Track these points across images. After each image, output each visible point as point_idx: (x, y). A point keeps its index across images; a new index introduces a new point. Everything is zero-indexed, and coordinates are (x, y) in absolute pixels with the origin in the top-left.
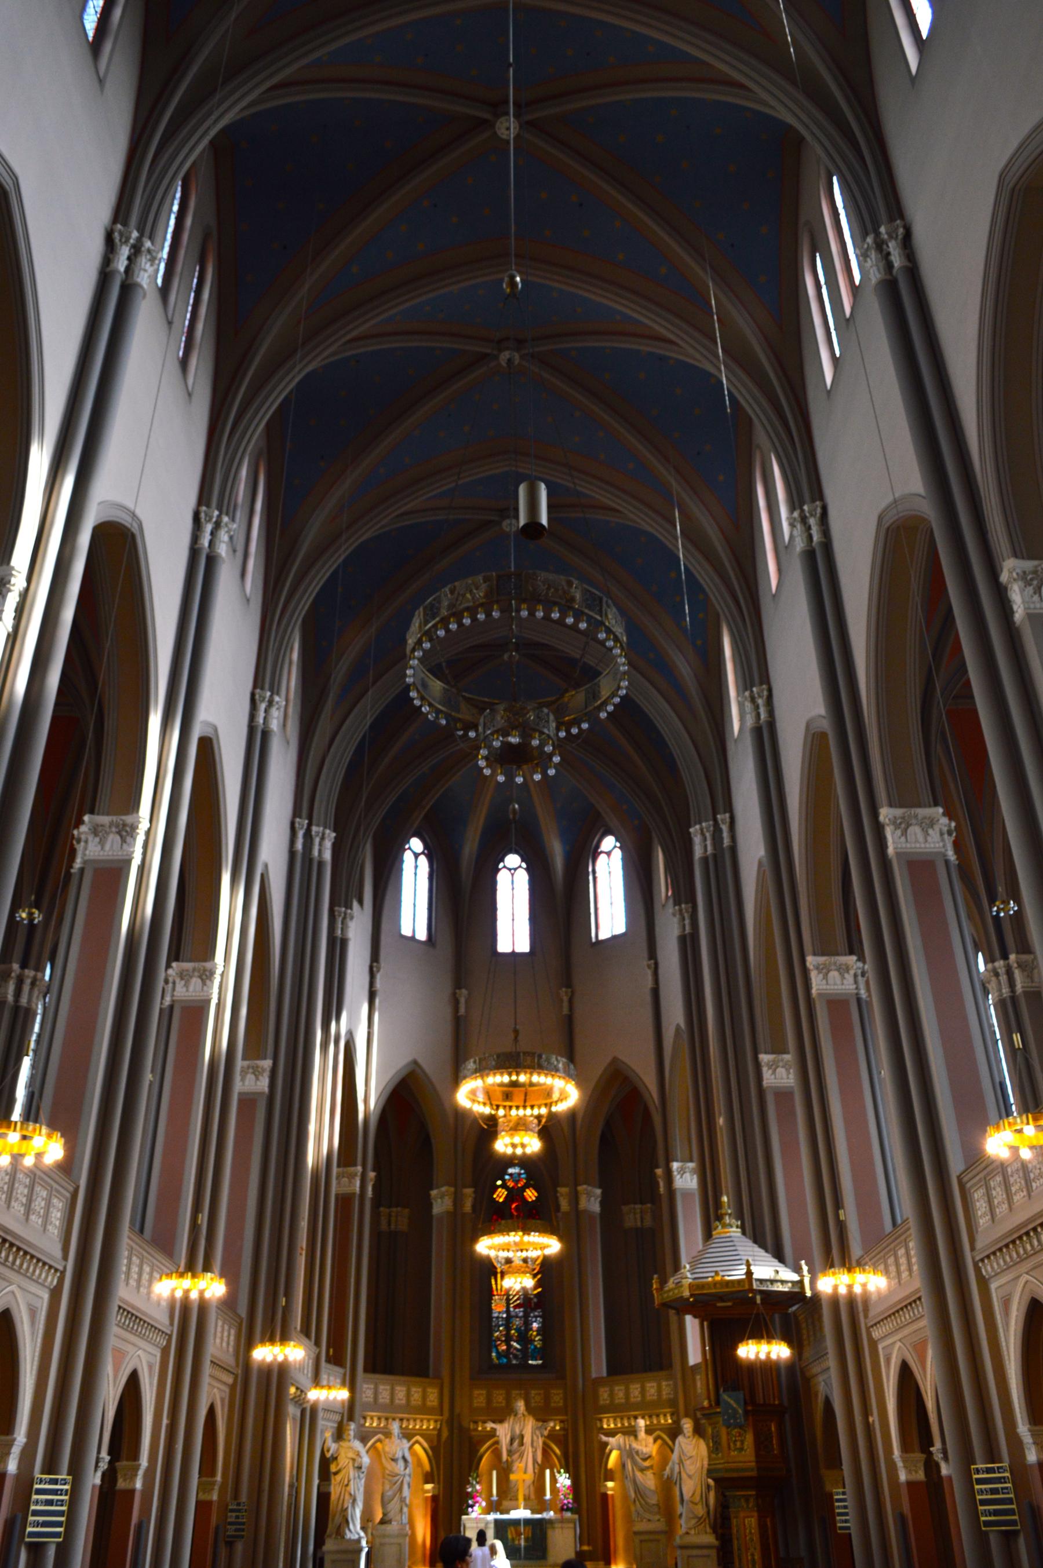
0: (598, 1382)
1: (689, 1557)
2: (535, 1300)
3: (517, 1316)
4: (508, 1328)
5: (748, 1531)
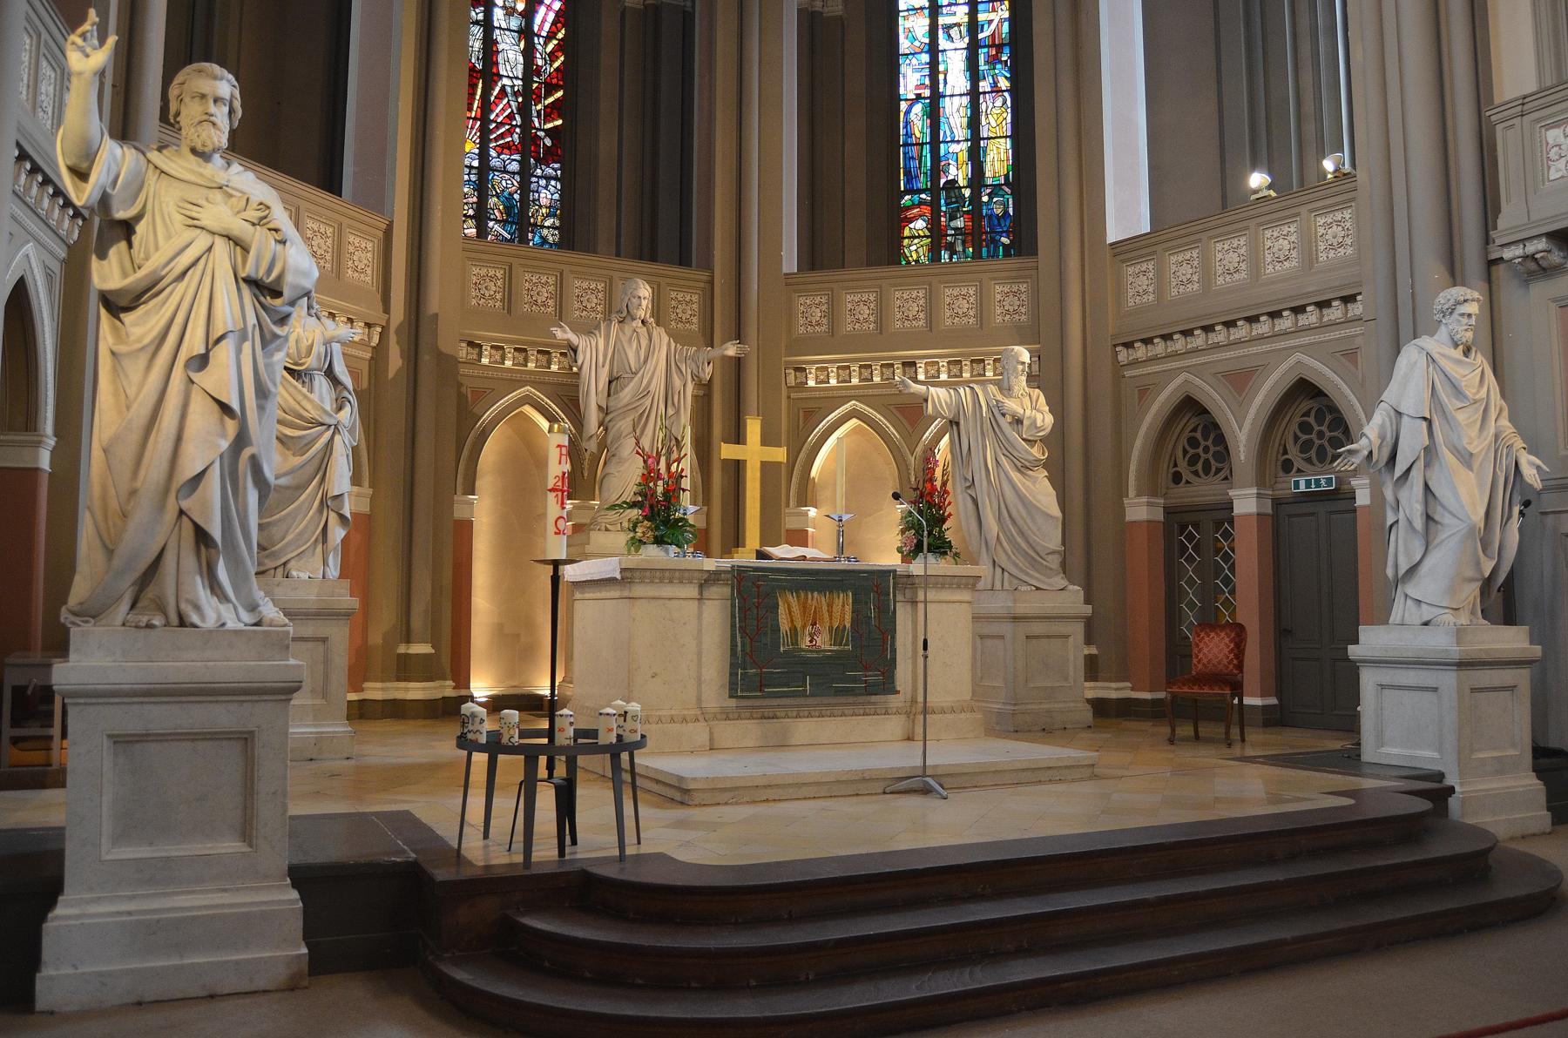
2: (548, 142)
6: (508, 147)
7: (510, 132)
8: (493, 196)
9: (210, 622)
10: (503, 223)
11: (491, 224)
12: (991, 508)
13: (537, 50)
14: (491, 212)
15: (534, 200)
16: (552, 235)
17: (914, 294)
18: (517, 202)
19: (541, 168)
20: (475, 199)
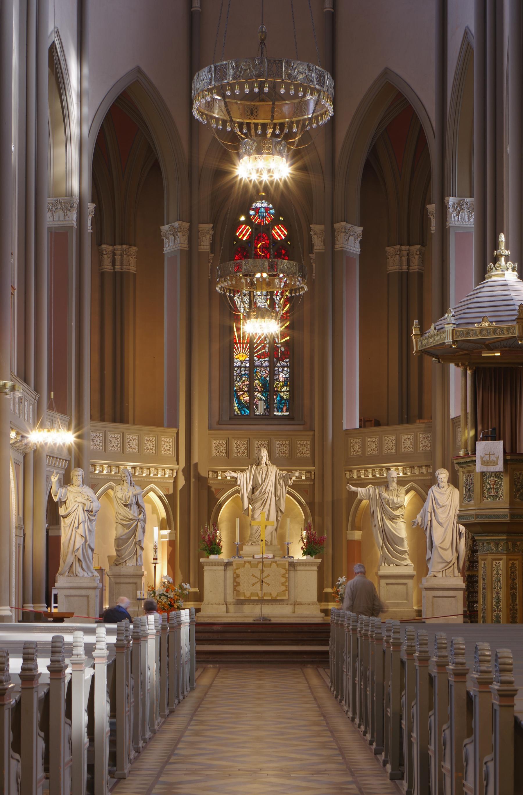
0: (350, 433)
1: (434, 597)
2: (283, 349)
3: (262, 366)
4: (251, 376)
5: (495, 572)
6: (264, 355)
7: (264, 347)
8: (257, 380)
9: (81, 575)
10: (262, 392)
11: (256, 393)
13: (276, 303)
14: (256, 387)
15: (277, 379)
16: (286, 395)
17: (392, 438)
18: (268, 381)
19: (279, 363)
20: (248, 383)
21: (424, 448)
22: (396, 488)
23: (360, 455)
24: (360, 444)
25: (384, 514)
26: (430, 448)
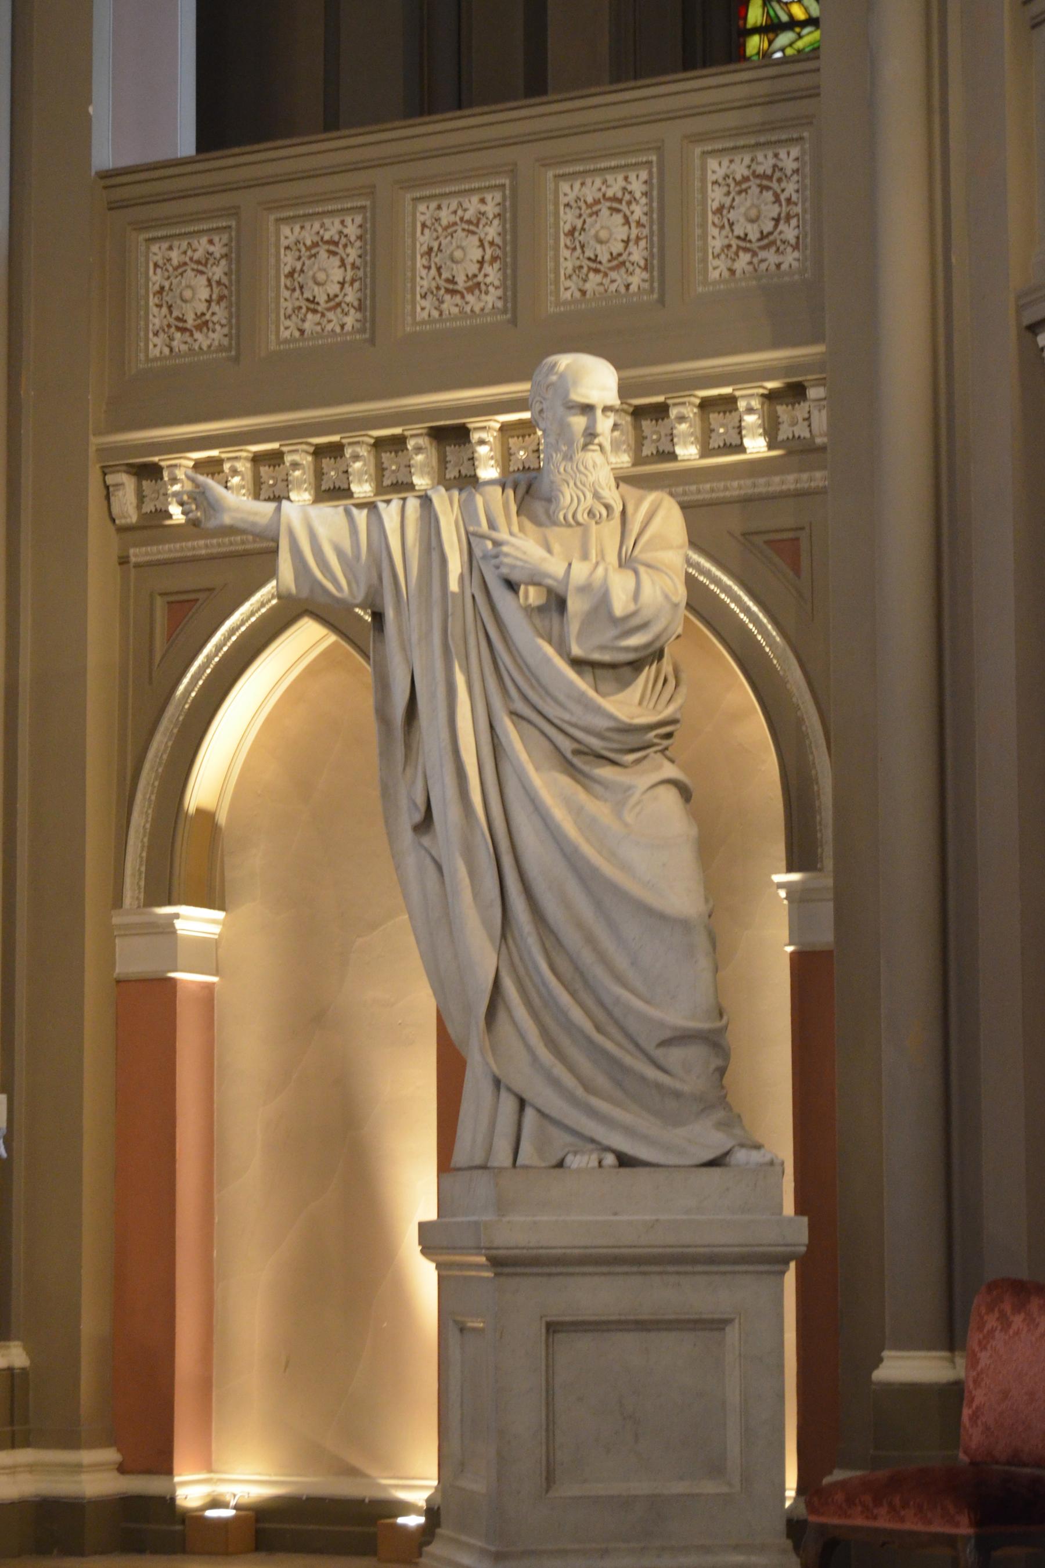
12: (476, 895)
17: (472, 206)
21: (745, 258)
22: (612, 495)
23: (221, 348)
24: (218, 272)
25: (514, 714)
26: (790, 258)
